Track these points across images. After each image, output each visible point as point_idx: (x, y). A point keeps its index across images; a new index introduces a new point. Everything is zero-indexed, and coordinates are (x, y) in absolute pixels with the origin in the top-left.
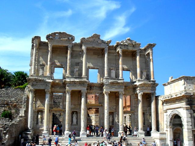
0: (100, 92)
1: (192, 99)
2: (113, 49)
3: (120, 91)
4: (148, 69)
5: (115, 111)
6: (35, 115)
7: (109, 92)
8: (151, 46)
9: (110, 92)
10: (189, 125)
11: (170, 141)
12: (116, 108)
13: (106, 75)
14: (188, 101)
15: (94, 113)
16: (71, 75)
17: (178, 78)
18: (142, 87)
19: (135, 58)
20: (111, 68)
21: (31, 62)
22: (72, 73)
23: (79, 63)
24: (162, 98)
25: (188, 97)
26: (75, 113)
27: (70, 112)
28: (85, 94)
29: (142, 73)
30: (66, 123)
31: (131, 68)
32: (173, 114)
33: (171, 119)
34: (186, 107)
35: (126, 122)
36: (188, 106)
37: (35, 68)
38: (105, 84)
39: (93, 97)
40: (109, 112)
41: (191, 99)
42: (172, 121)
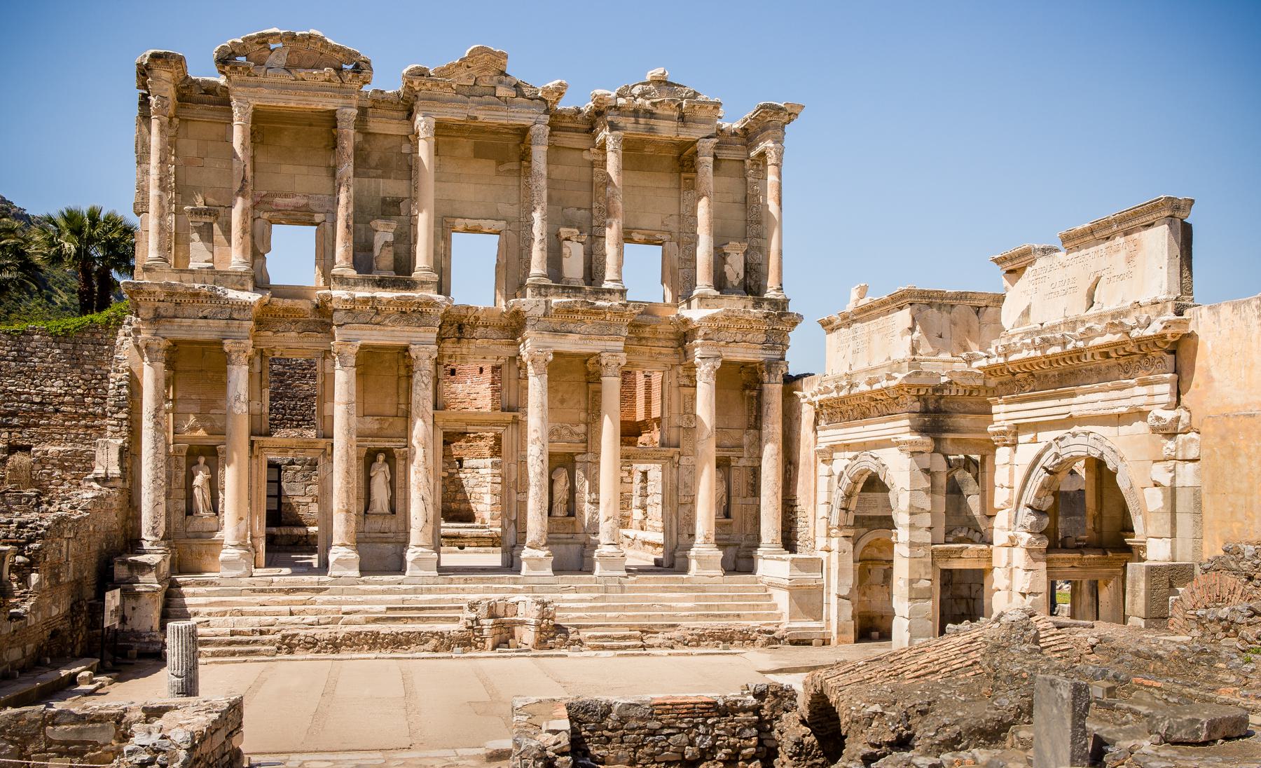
0: (508, 351)
2: (576, 130)
4: (759, 236)
5: (582, 450)
6: (177, 467)
7: (551, 358)
8: (771, 120)
9: (555, 354)
11: (840, 597)
12: (586, 434)
13: (537, 266)
14: (925, 412)
15: (487, 452)
16: (356, 265)
17: (885, 297)
18: (719, 330)
19: (693, 179)
20: (562, 230)
21: (143, 190)
22: (363, 259)
23: (396, 202)
24: (816, 388)
25: (922, 393)
26: (381, 457)
27: (353, 454)
30: (335, 508)
31: (670, 233)
32: (855, 470)
33: (848, 496)
34: (911, 443)
35: (649, 500)
36: (916, 437)
37: (162, 229)
38: (530, 314)
39: (481, 370)
40: (551, 455)
41: (937, 401)
42: (853, 506)
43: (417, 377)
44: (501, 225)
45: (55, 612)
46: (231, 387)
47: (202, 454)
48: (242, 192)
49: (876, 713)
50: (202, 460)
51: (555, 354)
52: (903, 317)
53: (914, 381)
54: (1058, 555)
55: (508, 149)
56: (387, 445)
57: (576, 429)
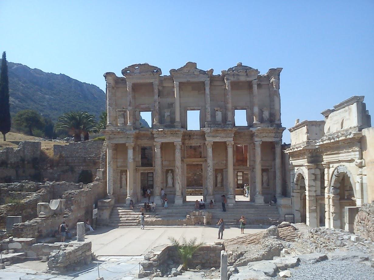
1: (318, 153)
3: (228, 141)
5: (225, 168)
7: (212, 144)
10: (312, 191)
20: (215, 108)
26: (170, 171)
28: (179, 146)
29: (263, 113)
43: (176, 150)
44: (199, 108)
45: (79, 215)
46: (128, 155)
47: (124, 172)
48: (130, 106)
49: (231, 254)
50: (124, 173)
51: (214, 142)
52: (304, 129)
53: (307, 148)
54: (346, 201)
55: (199, 87)
56: (171, 168)
57: (223, 162)
